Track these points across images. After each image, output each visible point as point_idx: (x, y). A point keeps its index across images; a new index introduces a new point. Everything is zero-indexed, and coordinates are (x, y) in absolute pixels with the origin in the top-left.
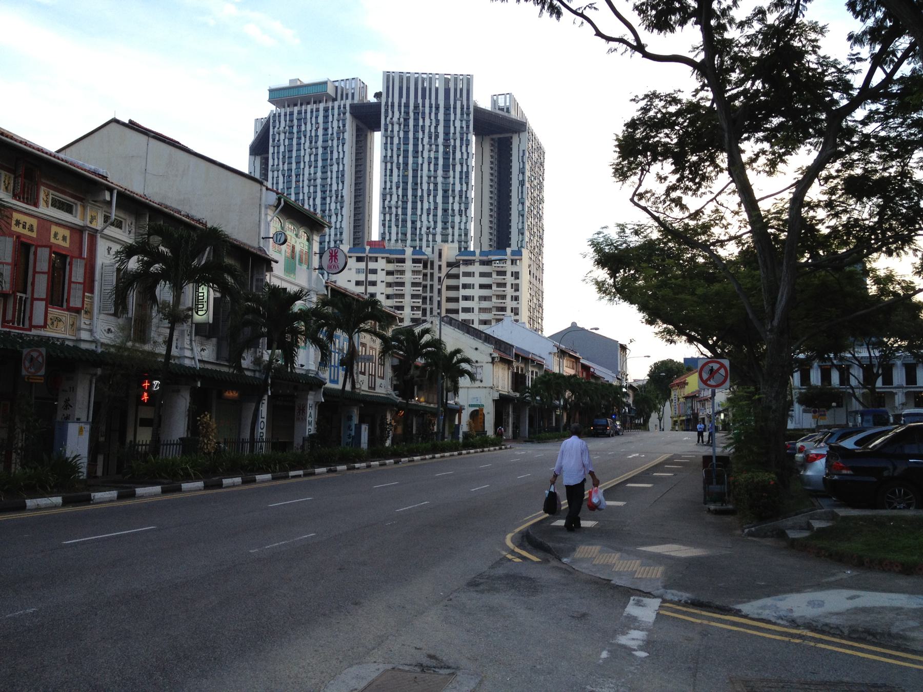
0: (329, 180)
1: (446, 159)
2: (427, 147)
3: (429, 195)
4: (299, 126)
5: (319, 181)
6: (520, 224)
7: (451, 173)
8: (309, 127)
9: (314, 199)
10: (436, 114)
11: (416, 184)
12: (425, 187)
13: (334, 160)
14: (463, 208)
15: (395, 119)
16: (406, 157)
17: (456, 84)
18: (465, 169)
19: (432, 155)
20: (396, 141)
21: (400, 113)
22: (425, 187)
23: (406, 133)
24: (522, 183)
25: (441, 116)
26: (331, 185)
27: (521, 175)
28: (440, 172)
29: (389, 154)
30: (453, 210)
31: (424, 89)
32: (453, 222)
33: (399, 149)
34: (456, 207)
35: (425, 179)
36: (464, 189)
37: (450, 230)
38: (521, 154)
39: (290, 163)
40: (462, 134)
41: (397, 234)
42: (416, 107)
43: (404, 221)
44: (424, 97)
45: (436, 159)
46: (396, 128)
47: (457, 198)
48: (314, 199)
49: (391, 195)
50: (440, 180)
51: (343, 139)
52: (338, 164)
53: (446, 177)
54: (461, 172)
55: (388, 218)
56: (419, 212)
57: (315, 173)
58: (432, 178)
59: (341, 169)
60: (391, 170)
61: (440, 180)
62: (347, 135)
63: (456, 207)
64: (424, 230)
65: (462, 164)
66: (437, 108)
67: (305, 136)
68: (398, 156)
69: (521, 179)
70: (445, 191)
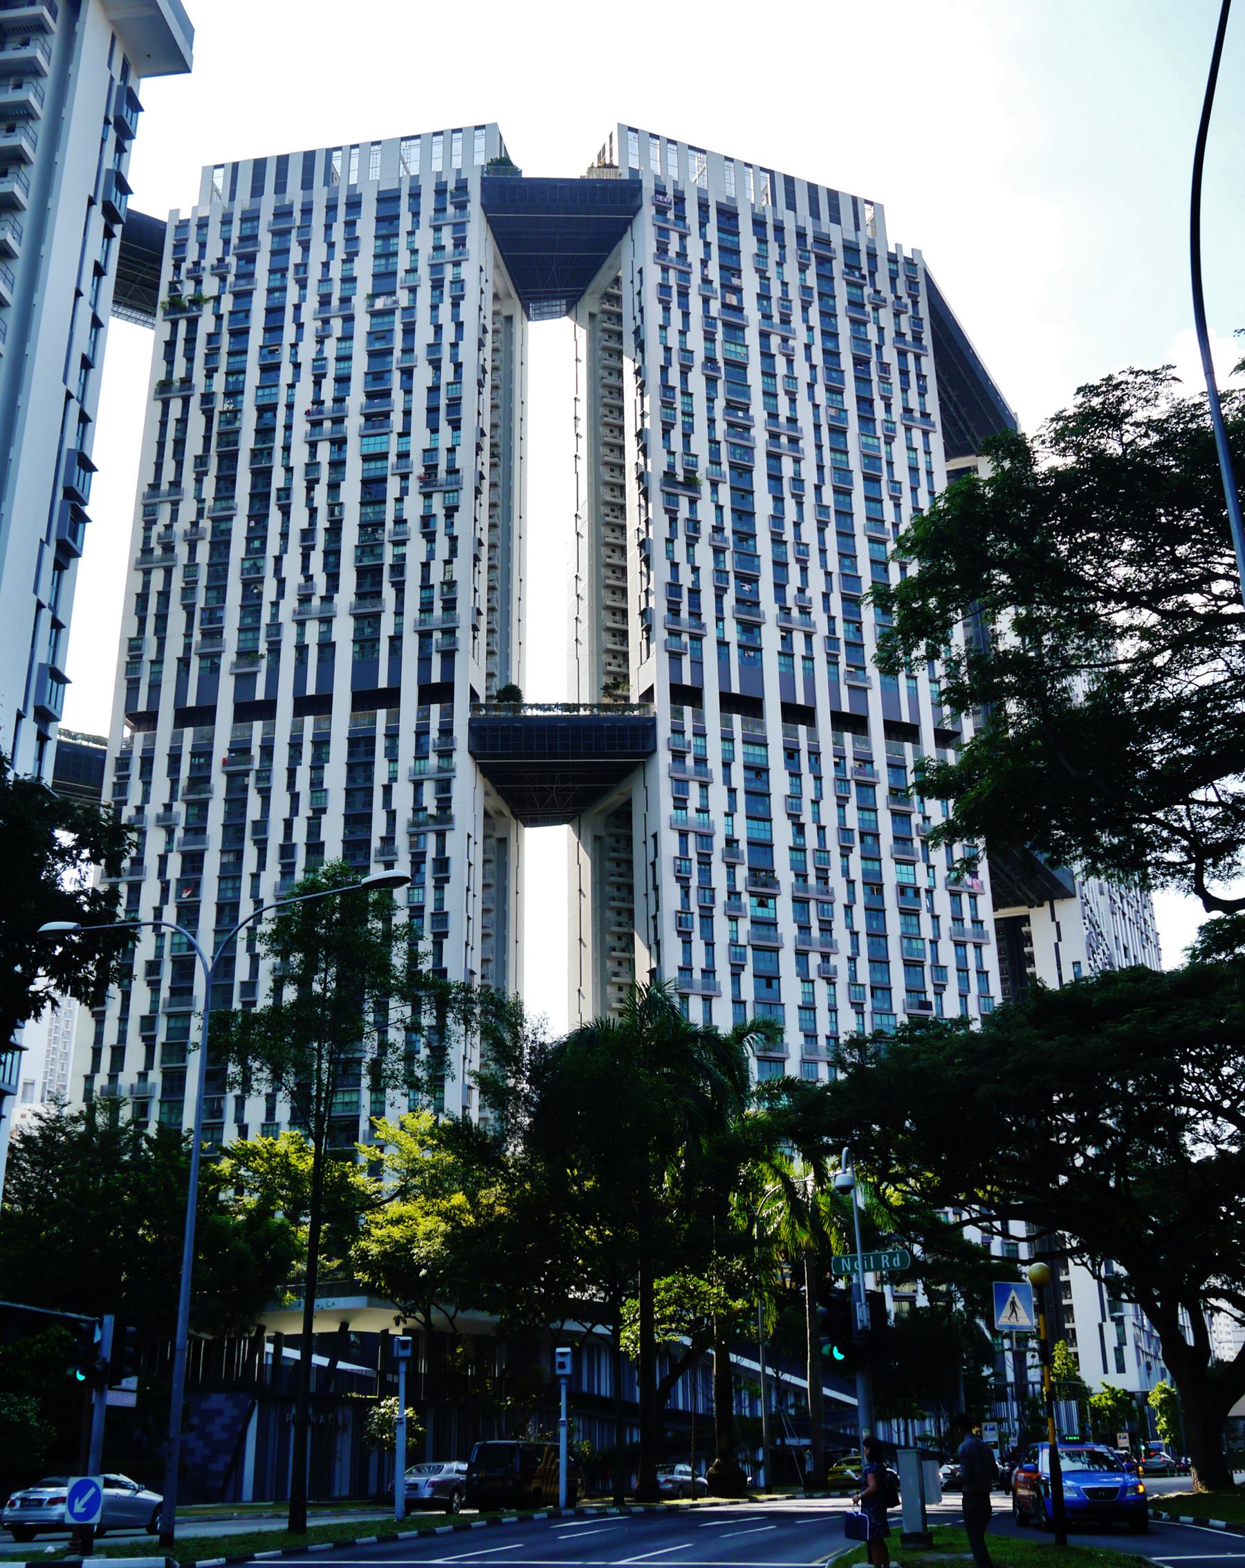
4: (280, 252)
8: (318, 252)
9: (334, 487)
39: (237, 372)
48: (334, 487)
51: (458, 283)
57: (339, 400)
62: (468, 272)
67: (302, 284)
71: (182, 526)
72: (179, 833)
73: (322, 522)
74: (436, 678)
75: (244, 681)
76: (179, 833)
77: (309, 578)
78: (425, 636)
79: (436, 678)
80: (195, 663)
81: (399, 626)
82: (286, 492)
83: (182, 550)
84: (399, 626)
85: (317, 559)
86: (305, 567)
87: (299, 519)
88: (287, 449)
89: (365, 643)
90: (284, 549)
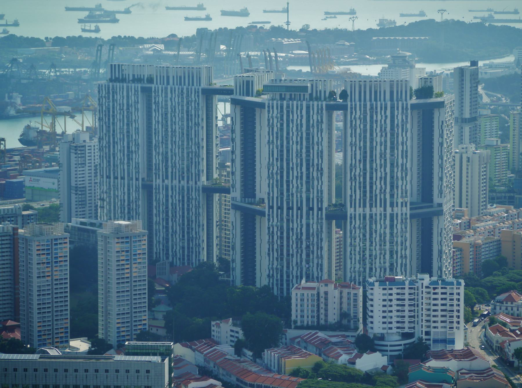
0: (311, 155)
1: (392, 143)
2: (379, 134)
3: (381, 168)
5: (304, 155)
6: (440, 174)
7: (396, 151)
10: (385, 113)
11: (372, 160)
12: (378, 162)
13: (315, 142)
14: (404, 175)
15: (357, 116)
16: (365, 142)
17: (397, 84)
18: (405, 149)
19: (383, 140)
20: (358, 131)
21: (361, 112)
22: (378, 162)
23: (365, 126)
24: (441, 144)
25: (388, 113)
26: (313, 160)
27: (440, 139)
28: (388, 151)
29: (354, 140)
30: (397, 177)
31: (376, 92)
32: (397, 184)
33: (360, 136)
34: (399, 174)
35: (378, 156)
36: (405, 162)
37: (395, 190)
38: (441, 124)
40: (403, 125)
41: (360, 194)
42: (372, 108)
43: (365, 187)
44: (376, 100)
45: (386, 142)
46: (358, 122)
47: (400, 169)
49: (356, 169)
50: (388, 156)
52: (318, 145)
53: (392, 155)
54: (402, 151)
55: (353, 184)
56: (374, 179)
58: (383, 155)
59: (320, 149)
60: (355, 151)
61: (388, 156)
63: (399, 174)
64: (378, 191)
65: (403, 145)
66: (386, 108)
68: (360, 141)
69: (440, 141)
70: (392, 165)
71: (275, 171)
72: (279, 228)
73: (299, 175)
74: (320, 206)
75: (288, 203)
76: (279, 228)
77: (298, 185)
78: (318, 199)
79: (320, 206)
80: (279, 198)
81: (313, 196)
82: (293, 168)
83: (275, 176)
84: (313, 196)
85: (299, 181)
86: (297, 183)
87: (295, 174)
88: (292, 159)
89: (308, 199)
90: (293, 178)
